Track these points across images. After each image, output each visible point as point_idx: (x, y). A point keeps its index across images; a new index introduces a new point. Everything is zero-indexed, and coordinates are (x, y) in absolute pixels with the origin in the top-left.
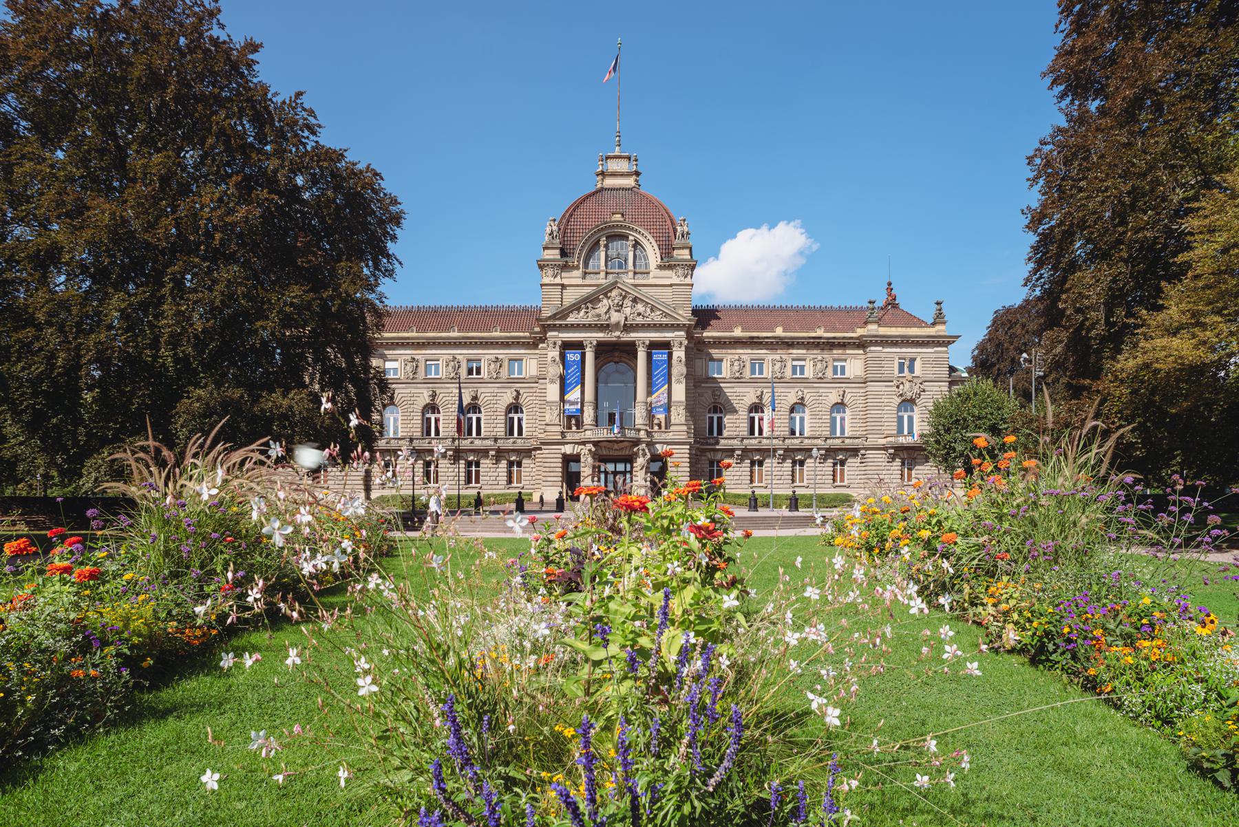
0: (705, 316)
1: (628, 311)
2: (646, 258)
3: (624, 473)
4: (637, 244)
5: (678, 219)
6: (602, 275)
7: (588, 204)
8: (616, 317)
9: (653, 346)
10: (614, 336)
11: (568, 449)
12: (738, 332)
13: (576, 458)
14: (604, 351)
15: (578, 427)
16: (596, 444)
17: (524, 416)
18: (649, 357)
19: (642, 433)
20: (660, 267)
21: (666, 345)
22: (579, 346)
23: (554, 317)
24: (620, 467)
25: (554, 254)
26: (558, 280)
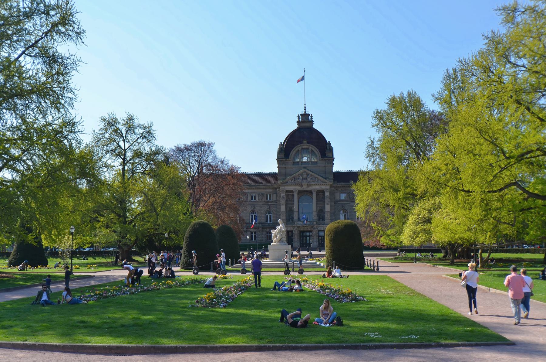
1: (309, 179)
3: (310, 236)
6: (300, 163)
9: (318, 191)
10: (305, 188)
13: (292, 231)
14: (301, 193)
15: (292, 221)
16: (298, 227)
18: (317, 195)
19: (315, 223)
21: (323, 191)
22: (292, 192)
24: (308, 234)
25: (283, 155)
26: (284, 166)
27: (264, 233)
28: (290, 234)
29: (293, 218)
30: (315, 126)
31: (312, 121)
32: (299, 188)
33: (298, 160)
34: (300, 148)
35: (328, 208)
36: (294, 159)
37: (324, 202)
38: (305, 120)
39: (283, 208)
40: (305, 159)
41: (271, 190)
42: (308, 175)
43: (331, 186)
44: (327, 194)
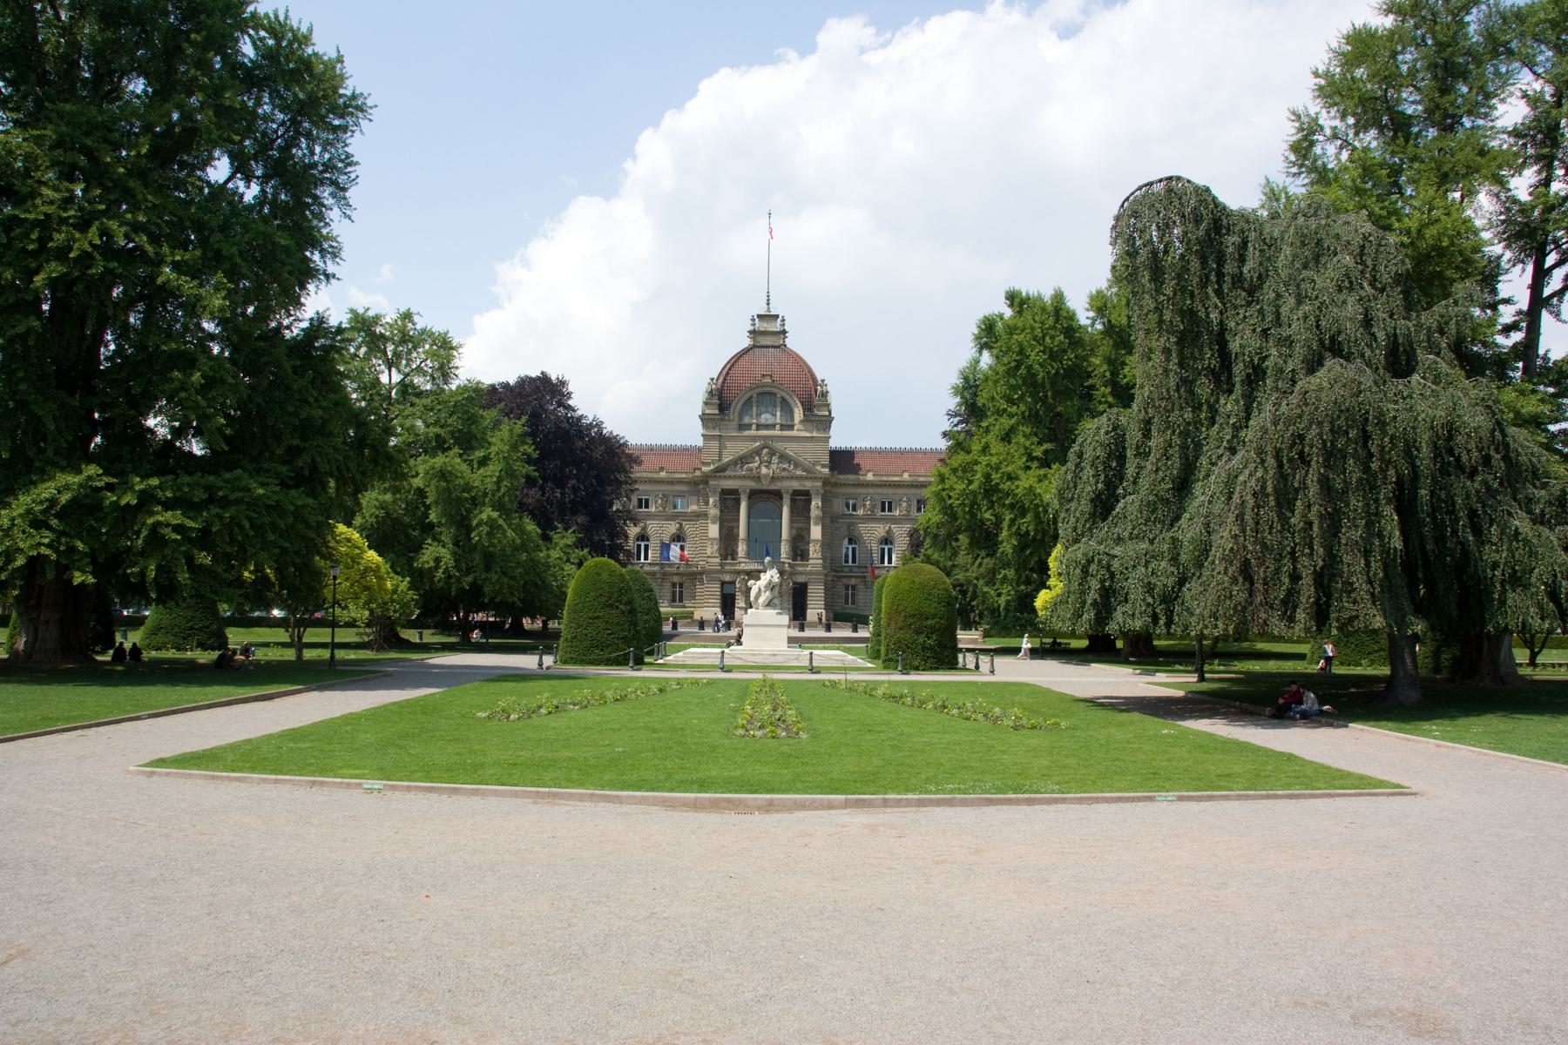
0: (843, 460)
1: (774, 467)
2: (792, 412)
4: (783, 400)
5: (819, 379)
7: (742, 362)
8: (764, 470)
9: (796, 493)
10: (765, 485)
11: (727, 578)
12: (870, 477)
14: (754, 495)
17: (687, 546)
18: (793, 501)
20: (801, 422)
22: (735, 492)
23: (717, 470)
27: (668, 586)
28: (728, 590)
29: (734, 555)
30: (791, 343)
31: (784, 332)
32: (752, 484)
33: (746, 420)
34: (754, 393)
35: (816, 532)
36: (740, 418)
37: (809, 518)
38: (767, 334)
39: (714, 530)
40: (766, 418)
41: (684, 488)
42: (772, 453)
43: (825, 484)
44: (816, 503)
